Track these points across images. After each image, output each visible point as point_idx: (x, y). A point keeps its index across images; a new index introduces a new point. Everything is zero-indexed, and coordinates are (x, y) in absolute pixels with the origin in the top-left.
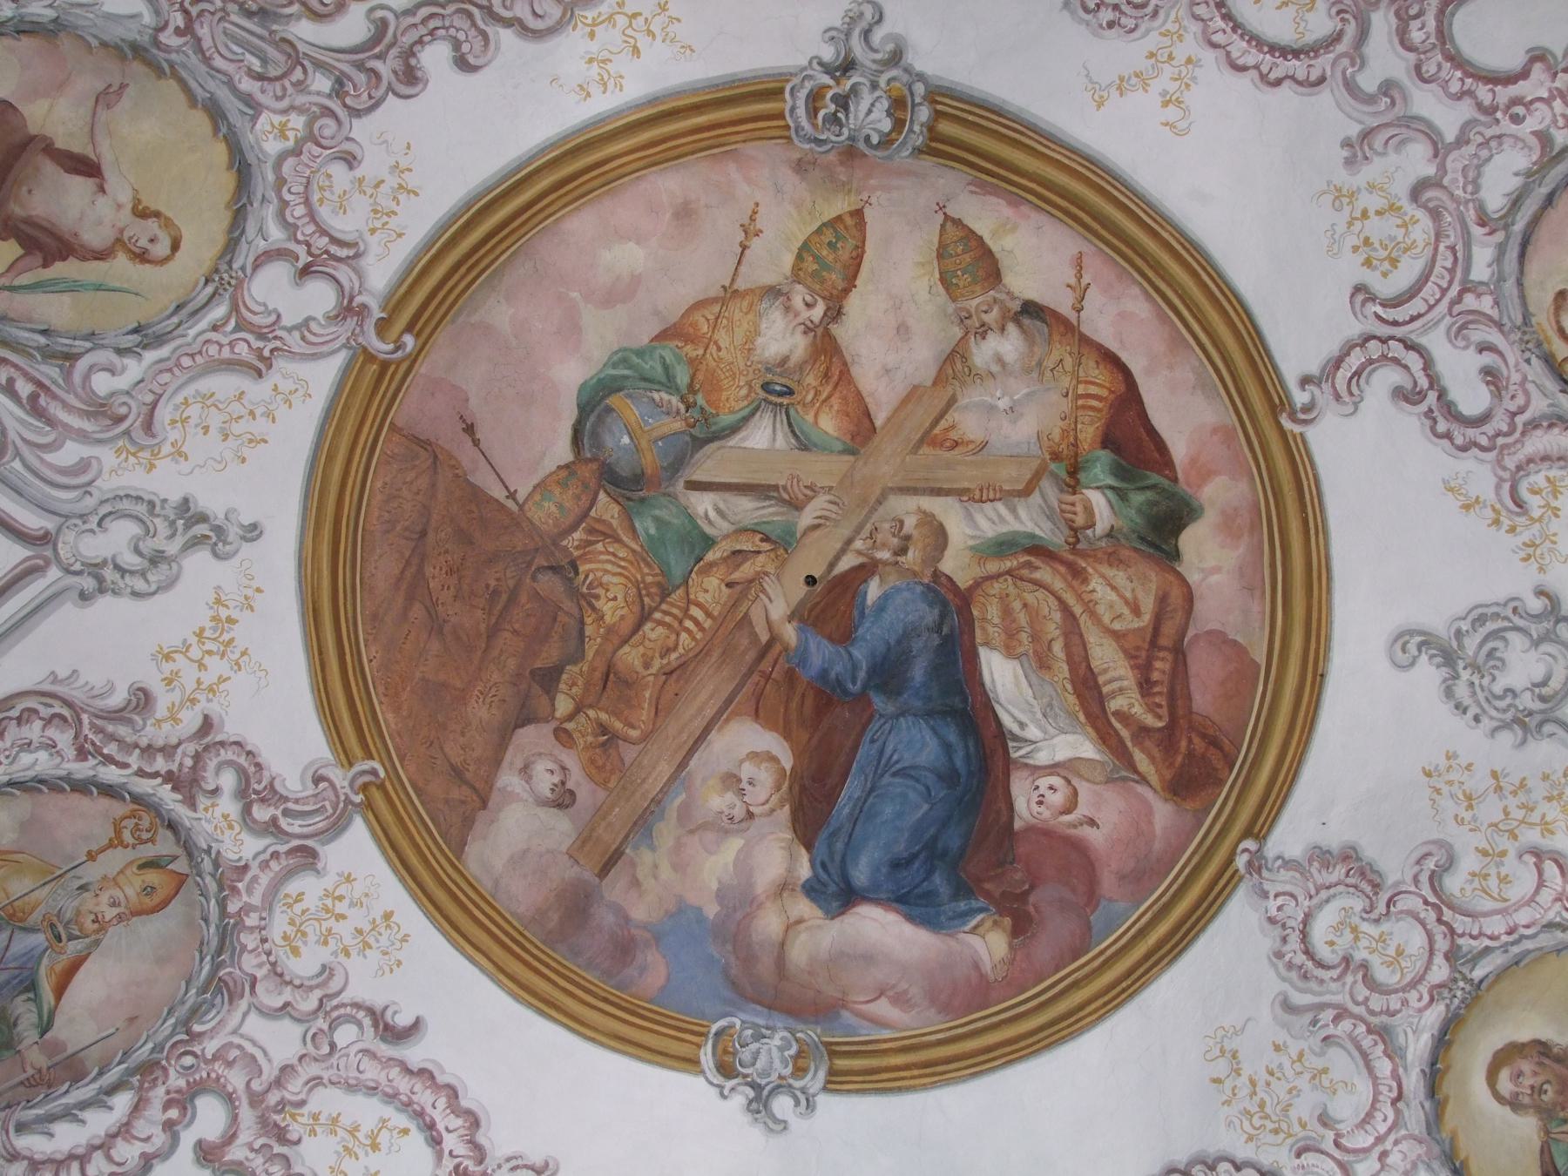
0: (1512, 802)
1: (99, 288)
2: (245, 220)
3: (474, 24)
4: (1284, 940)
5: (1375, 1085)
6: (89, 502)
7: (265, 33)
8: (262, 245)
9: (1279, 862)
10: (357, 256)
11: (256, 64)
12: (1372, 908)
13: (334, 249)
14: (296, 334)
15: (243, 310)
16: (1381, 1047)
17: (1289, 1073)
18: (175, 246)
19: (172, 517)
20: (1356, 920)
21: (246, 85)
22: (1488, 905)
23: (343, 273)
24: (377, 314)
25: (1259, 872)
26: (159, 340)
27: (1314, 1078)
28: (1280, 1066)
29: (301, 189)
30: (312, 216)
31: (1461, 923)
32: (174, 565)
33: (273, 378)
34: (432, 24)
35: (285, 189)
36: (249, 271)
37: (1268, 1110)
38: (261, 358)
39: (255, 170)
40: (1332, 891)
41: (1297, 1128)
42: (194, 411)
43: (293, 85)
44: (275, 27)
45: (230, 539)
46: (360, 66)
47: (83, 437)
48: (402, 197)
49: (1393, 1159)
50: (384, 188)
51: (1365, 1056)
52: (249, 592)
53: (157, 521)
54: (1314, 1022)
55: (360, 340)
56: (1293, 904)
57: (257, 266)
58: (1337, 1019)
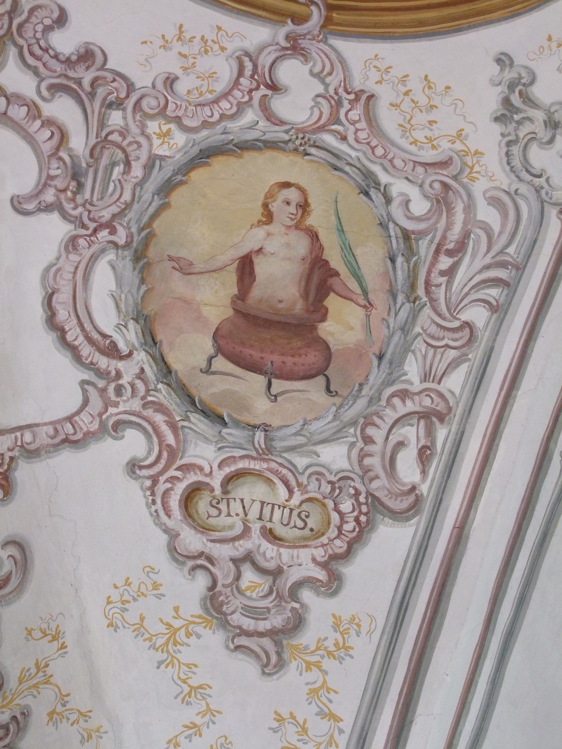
1: (341, 230)
2: (247, 141)
3: (27, 21)
6: (523, 189)
7: (91, 170)
8: (263, 124)
10: (247, 54)
11: (118, 170)
13: (248, 71)
14: (328, 80)
15: (322, 122)
18: (286, 185)
19: (514, 125)
21: (137, 171)
23: (265, 60)
24: (290, 26)
26: (368, 175)
29: (207, 110)
30: (225, 95)
32: (552, 110)
33: (371, 86)
34: (39, 52)
35: (210, 120)
36: (287, 127)
38: (357, 99)
39: (203, 145)
42: (419, 135)
43: (124, 138)
44: (84, 165)
45: (516, 76)
46: (92, 95)
47: (470, 208)
48: (188, 36)
50: (185, 50)
52: (554, 45)
53: (521, 135)
55: (316, 32)
57: (282, 123)
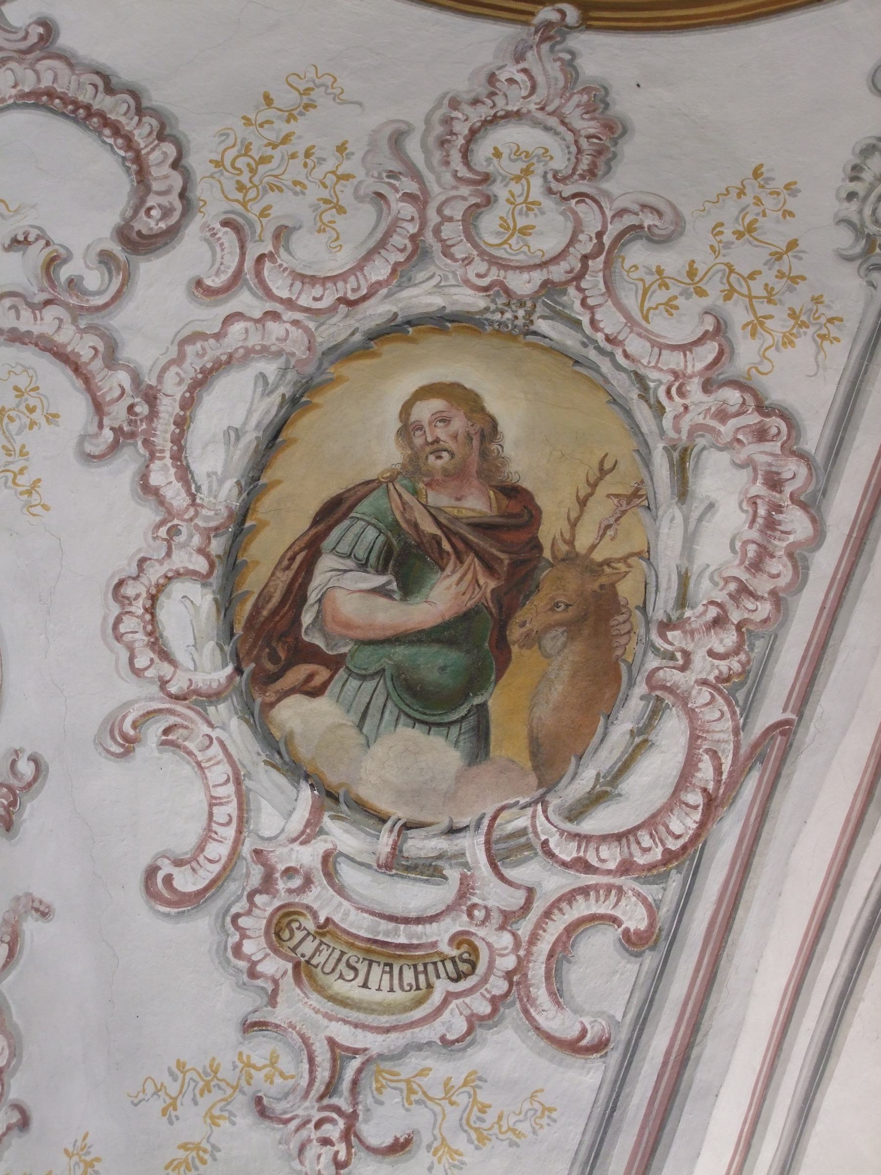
0: (768, 277)
4: (476, 102)
5: (352, 271)
9: (567, 57)
12: (563, 180)
16: (401, 258)
17: (318, 173)
20: (539, 168)
22: (631, 302)
25: (543, 40)
27: (326, 201)
28: (321, 160)
31: (594, 282)
37: (262, 169)
40: (562, 129)
41: (256, 208)
49: (275, 329)
51: (382, 244)
54: (392, 175)
56: (524, 93)
58: (409, 197)
